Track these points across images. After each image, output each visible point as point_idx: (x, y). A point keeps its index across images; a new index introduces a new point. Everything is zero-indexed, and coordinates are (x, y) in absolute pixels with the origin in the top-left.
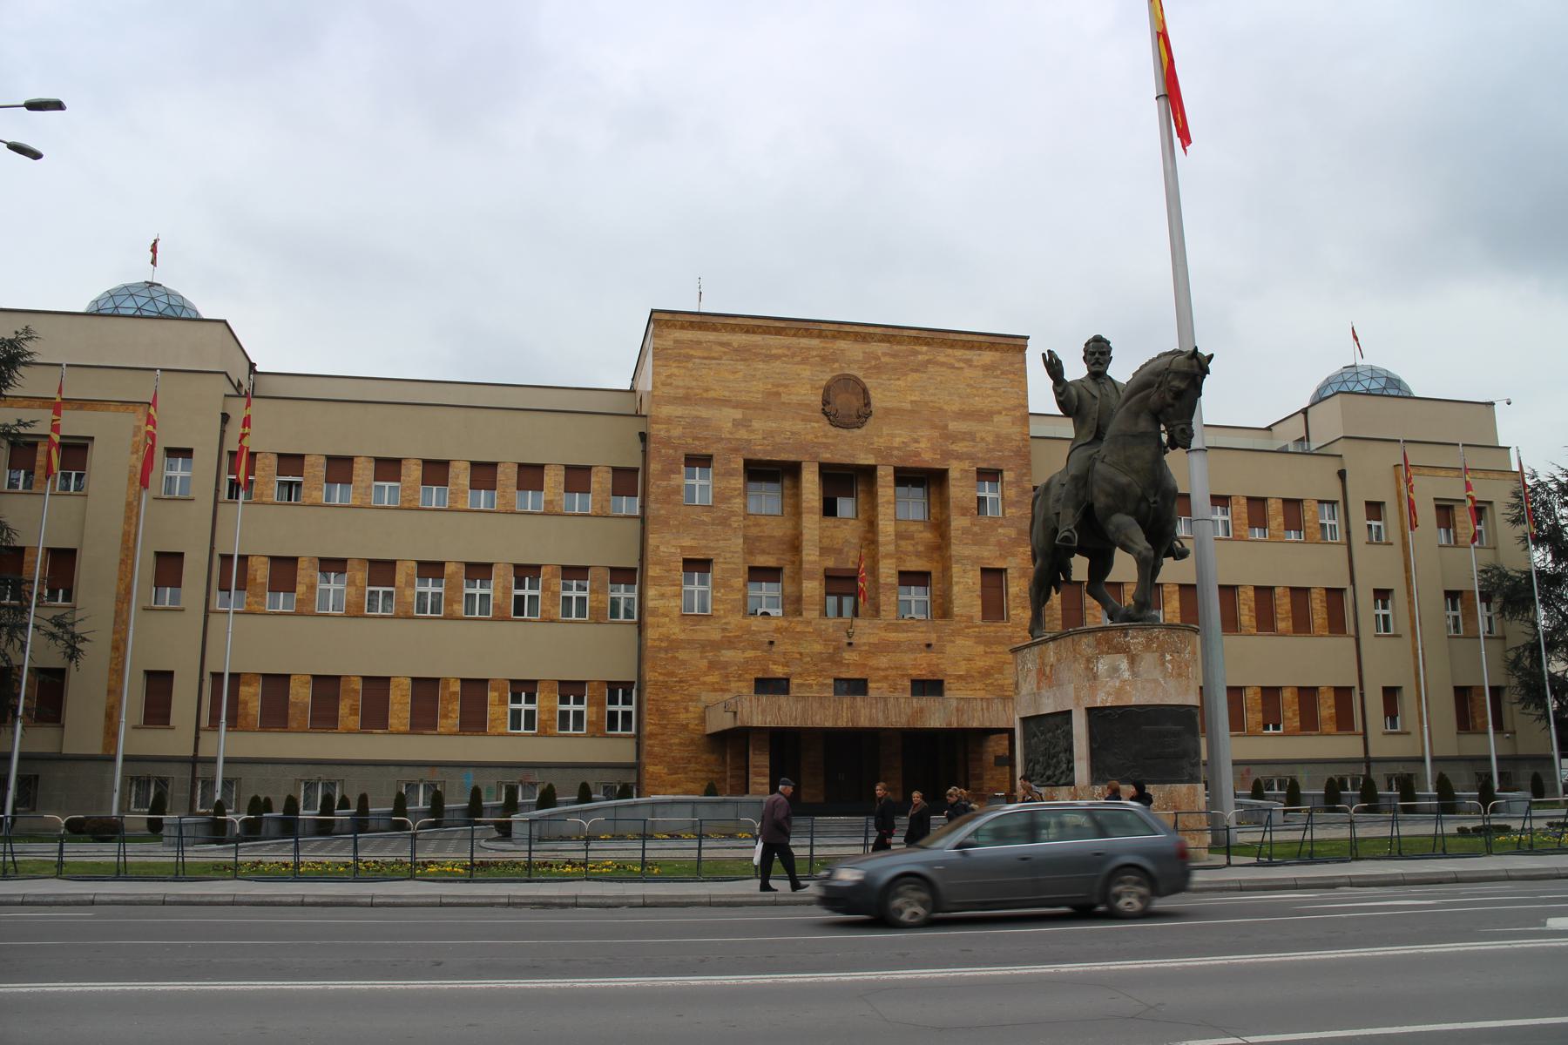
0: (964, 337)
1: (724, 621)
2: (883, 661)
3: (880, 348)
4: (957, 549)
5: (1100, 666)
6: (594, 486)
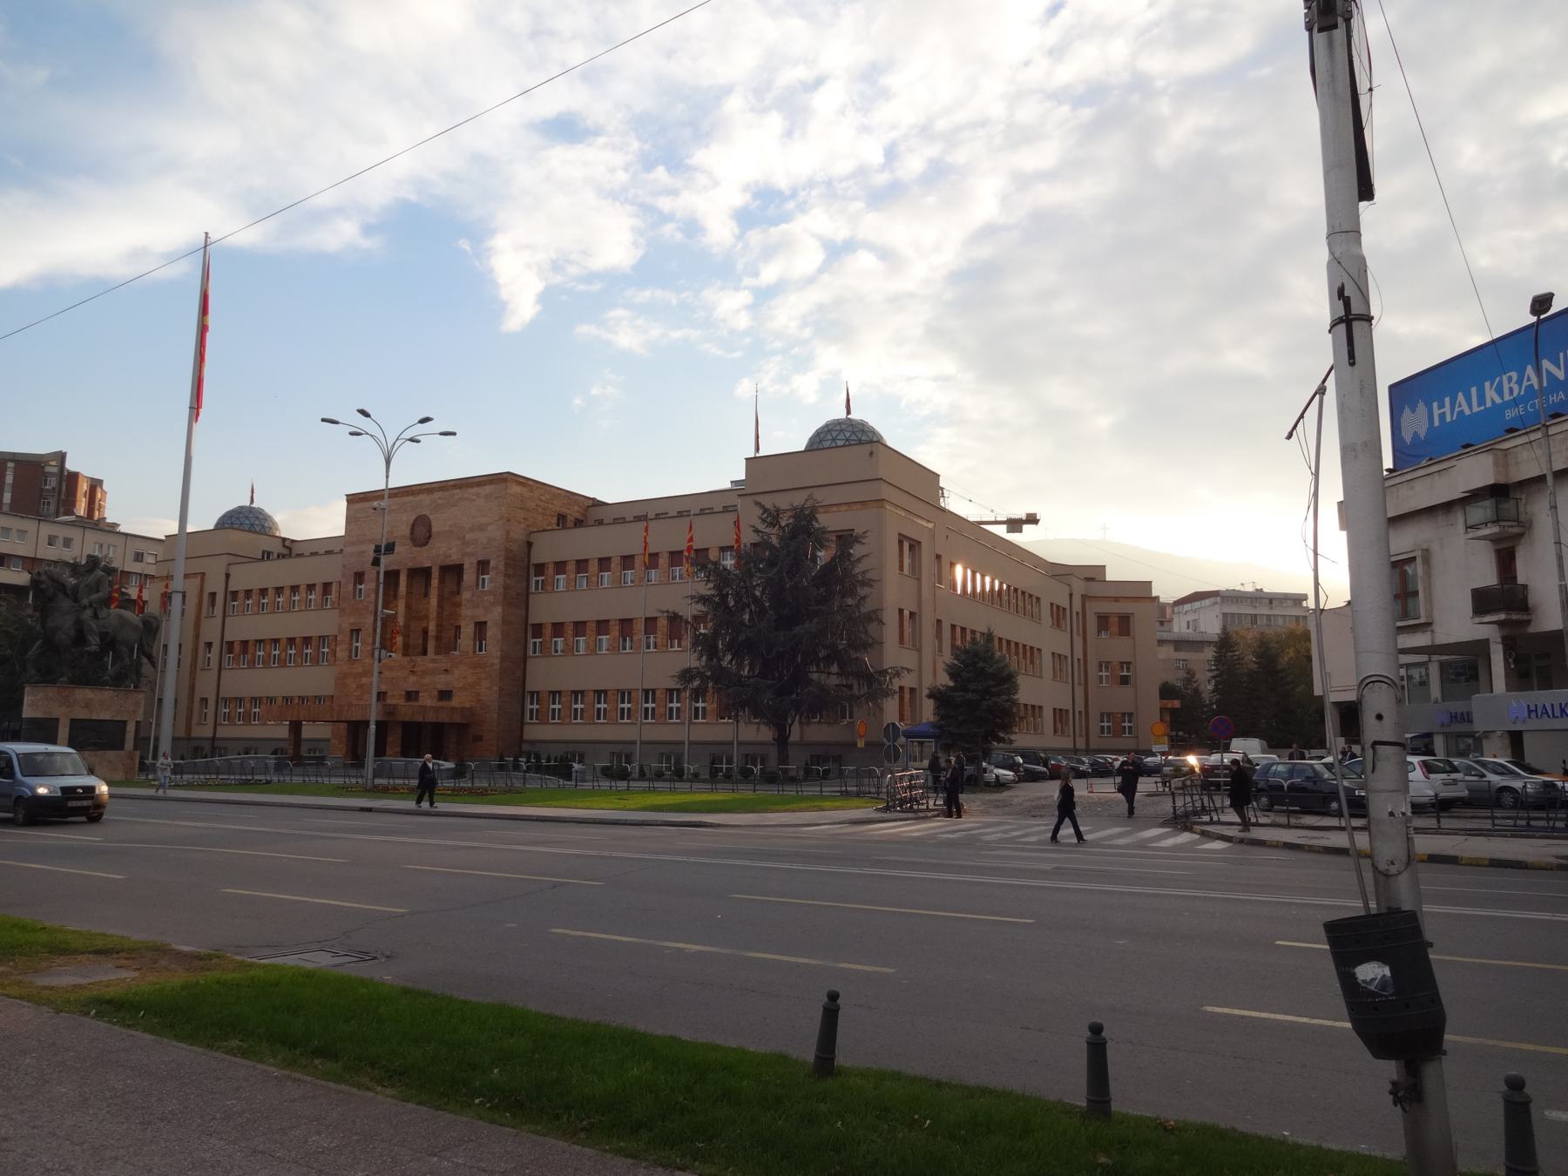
0: (477, 480)
2: (426, 680)
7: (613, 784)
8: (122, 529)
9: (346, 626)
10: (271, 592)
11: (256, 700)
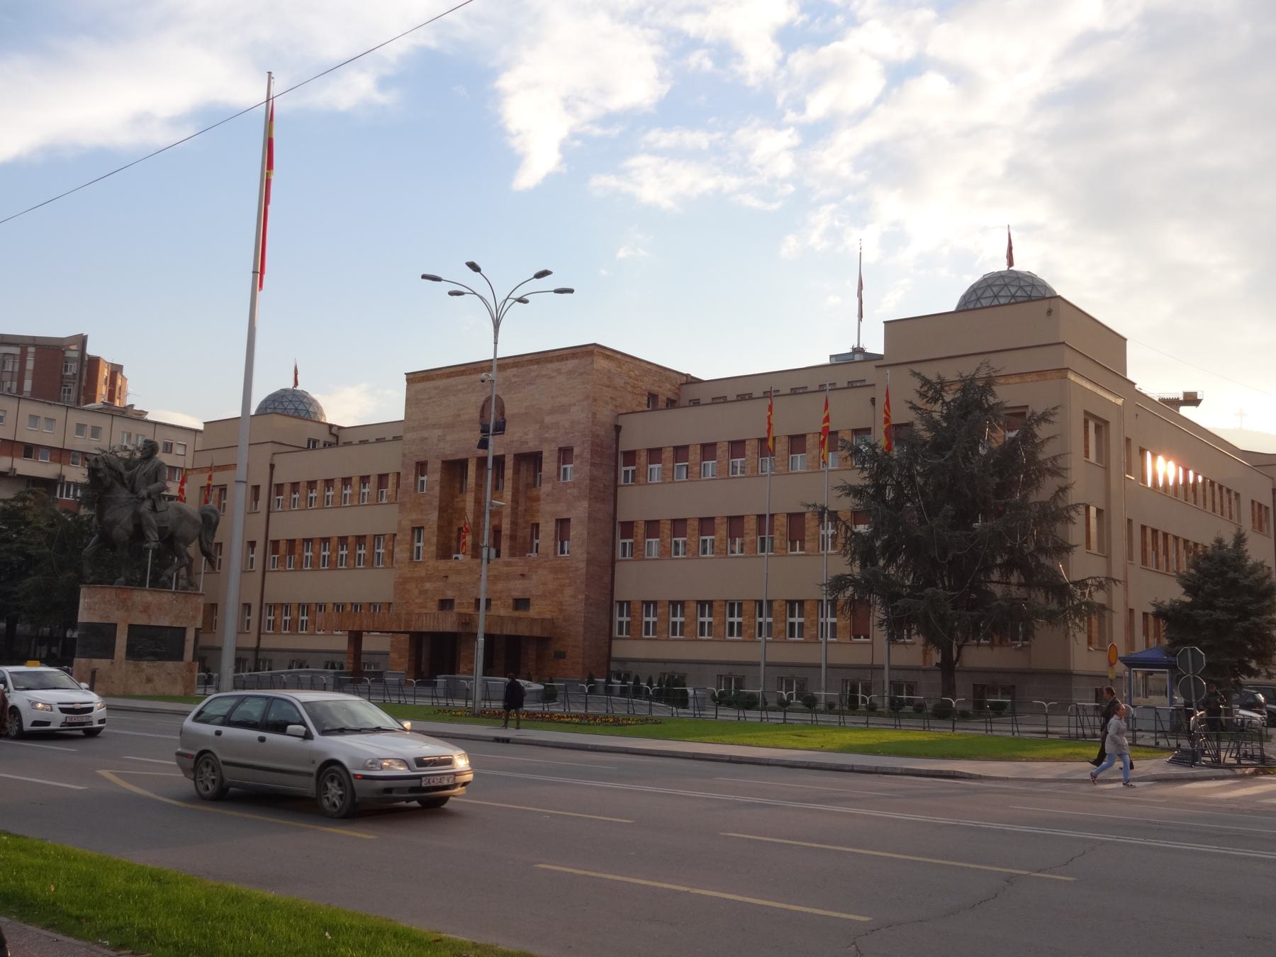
0: (557, 353)
7: (741, 714)
8: (149, 417)
9: (407, 524)
10: (320, 486)
11: (303, 607)
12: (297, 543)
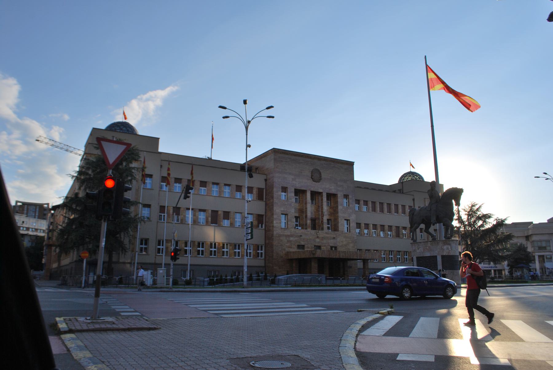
1: (290, 230)
2: (325, 241)
3: (323, 162)
4: (340, 214)
5: (445, 247)
6: (254, 192)
12: (181, 209)
